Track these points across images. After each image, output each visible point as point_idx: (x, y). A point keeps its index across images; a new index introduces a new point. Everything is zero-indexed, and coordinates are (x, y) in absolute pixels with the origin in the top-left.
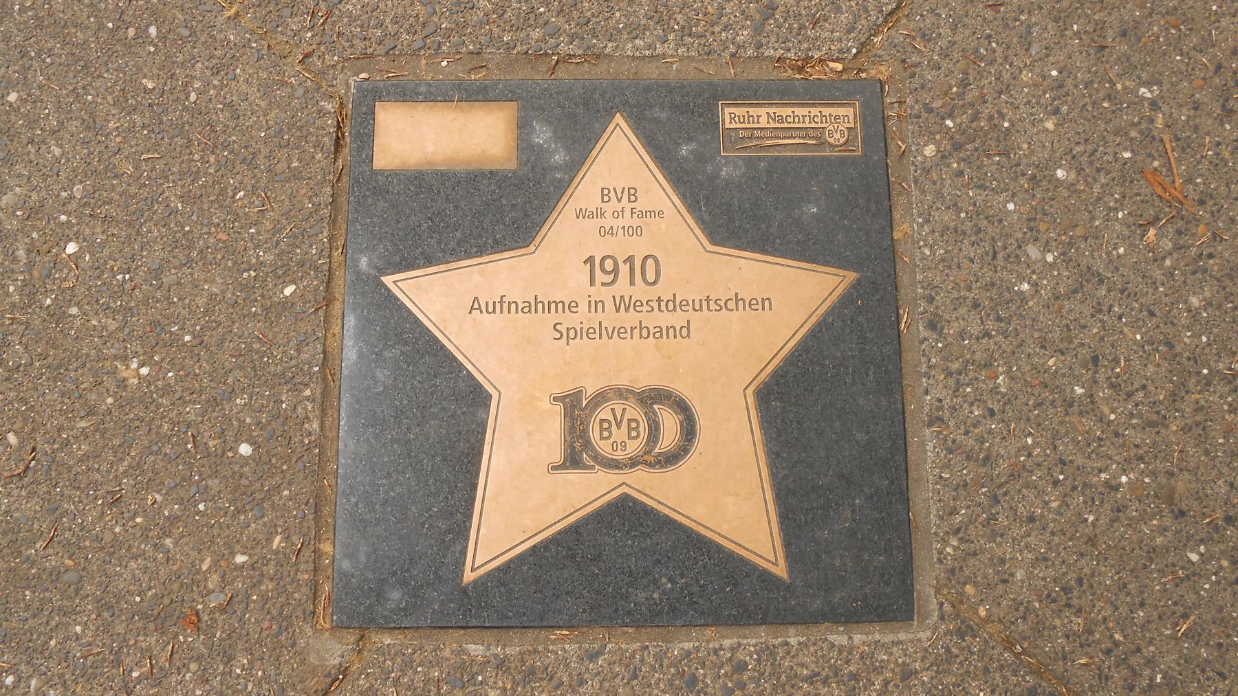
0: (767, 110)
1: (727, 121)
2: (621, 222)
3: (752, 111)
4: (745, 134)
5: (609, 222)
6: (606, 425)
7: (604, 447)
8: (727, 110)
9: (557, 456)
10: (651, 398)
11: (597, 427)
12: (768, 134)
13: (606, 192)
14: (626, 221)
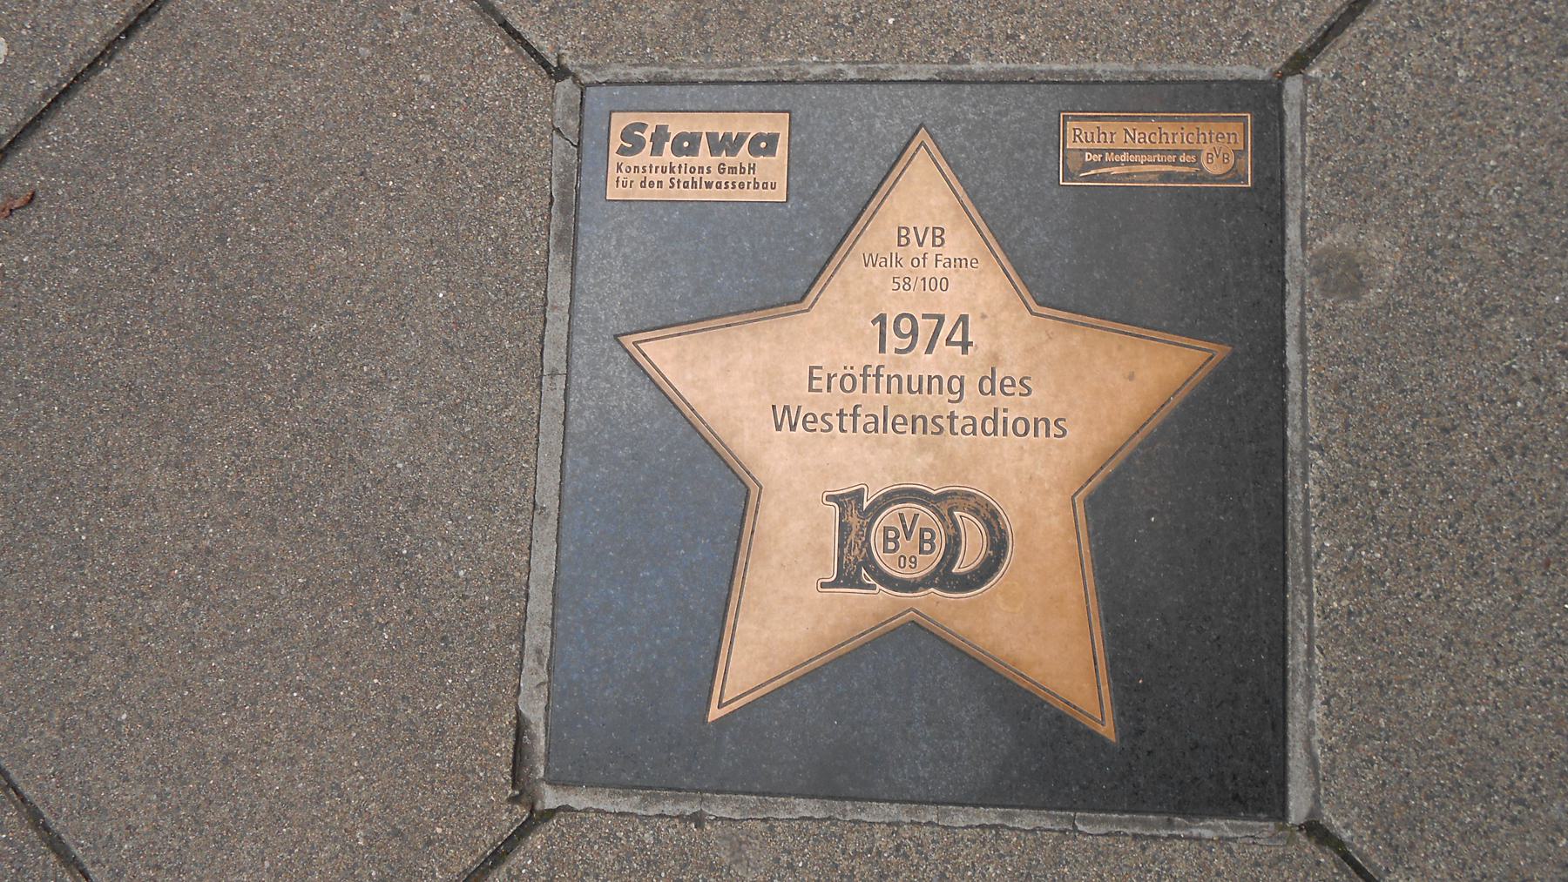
1: (1070, 138)
4: (1097, 158)
5: (904, 270)
6: (891, 534)
8: (1071, 125)
11: (880, 536)
12: (1124, 157)
13: (904, 232)
14: (932, 271)
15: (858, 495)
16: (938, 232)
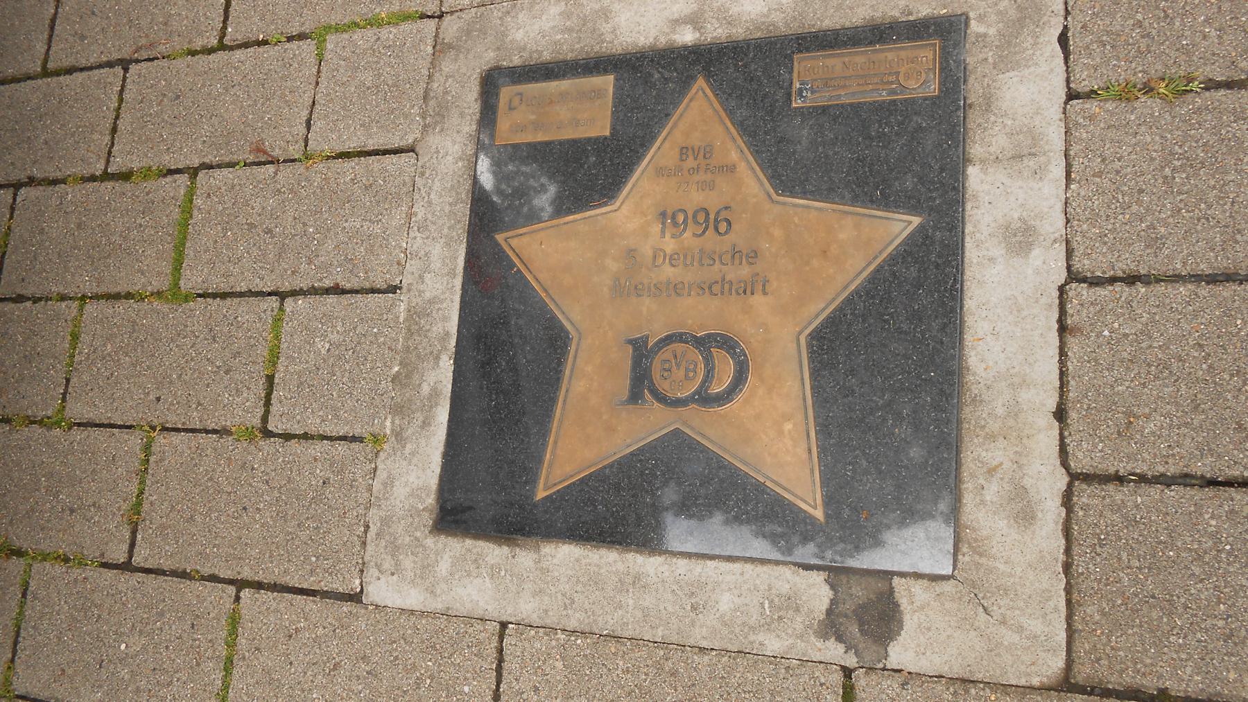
7: (664, 386)
9: (625, 394)
10: (703, 343)
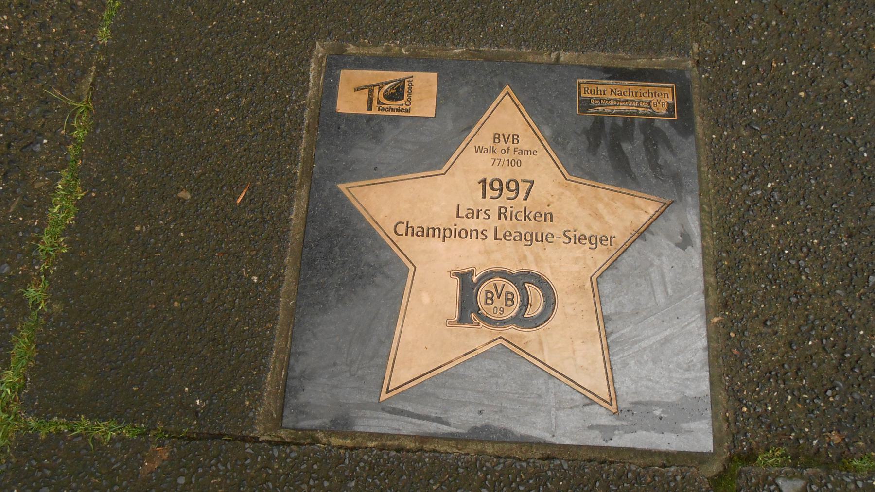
0: (611, 87)
2: (506, 157)
3: (601, 87)
10: (521, 279)
11: (483, 294)
13: (497, 136)
15: (471, 273)
16: (516, 137)
